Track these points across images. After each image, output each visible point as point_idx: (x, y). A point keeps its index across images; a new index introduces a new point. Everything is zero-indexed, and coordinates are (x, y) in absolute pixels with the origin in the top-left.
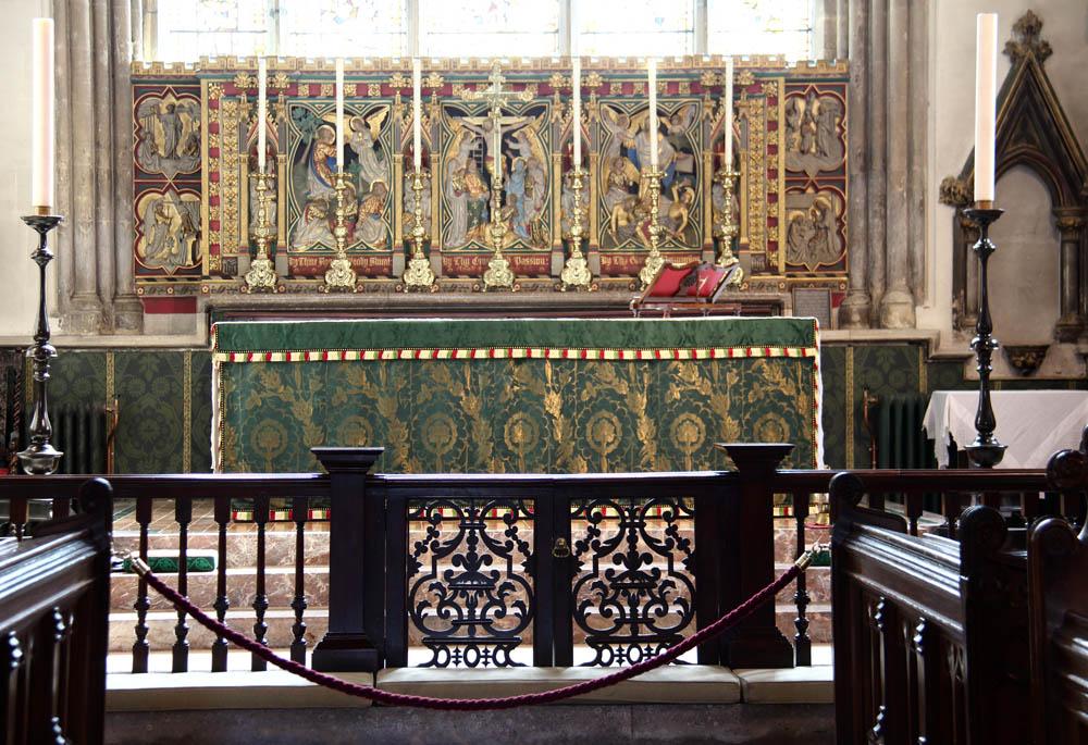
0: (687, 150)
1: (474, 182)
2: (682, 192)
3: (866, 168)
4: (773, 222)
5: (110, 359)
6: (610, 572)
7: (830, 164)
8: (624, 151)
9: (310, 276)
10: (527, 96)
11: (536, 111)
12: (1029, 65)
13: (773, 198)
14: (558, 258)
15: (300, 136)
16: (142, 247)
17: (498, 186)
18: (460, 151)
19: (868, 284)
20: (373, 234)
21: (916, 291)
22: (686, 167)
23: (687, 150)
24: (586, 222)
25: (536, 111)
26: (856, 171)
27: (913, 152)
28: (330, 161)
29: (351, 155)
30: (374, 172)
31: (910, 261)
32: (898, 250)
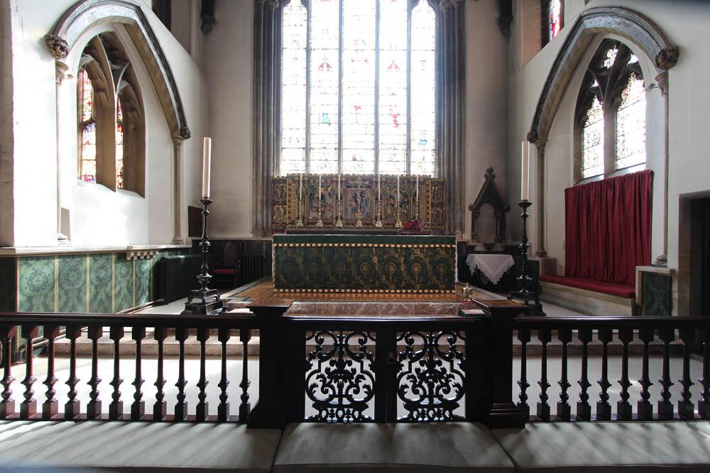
0: (406, 196)
1: (353, 203)
2: (405, 206)
3: (449, 202)
4: (428, 214)
5: (264, 243)
6: (418, 370)
7: (440, 201)
8: (391, 196)
9: (313, 224)
10: (367, 183)
11: (369, 187)
12: (491, 180)
13: (428, 208)
14: (374, 221)
15: (311, 192)
16: (274, 218)
17: (359, 203)
18: (350, 196)
19: (449, 228)
20: (328, 215)
21: (462, 230)
22: (406, 200)
23: (406, 196)
24: (381, 212)
25: (369, 187)
26: (447, 203)
27: (462, 198)
28: (318, 198)
29: (322, 196)
30: (329, 201)
31: (461, 223)
32: (458, 221)
